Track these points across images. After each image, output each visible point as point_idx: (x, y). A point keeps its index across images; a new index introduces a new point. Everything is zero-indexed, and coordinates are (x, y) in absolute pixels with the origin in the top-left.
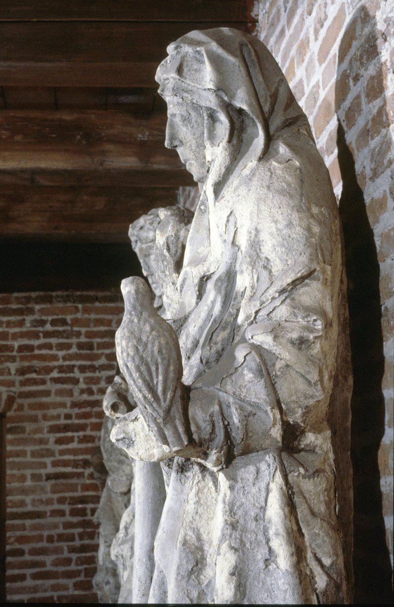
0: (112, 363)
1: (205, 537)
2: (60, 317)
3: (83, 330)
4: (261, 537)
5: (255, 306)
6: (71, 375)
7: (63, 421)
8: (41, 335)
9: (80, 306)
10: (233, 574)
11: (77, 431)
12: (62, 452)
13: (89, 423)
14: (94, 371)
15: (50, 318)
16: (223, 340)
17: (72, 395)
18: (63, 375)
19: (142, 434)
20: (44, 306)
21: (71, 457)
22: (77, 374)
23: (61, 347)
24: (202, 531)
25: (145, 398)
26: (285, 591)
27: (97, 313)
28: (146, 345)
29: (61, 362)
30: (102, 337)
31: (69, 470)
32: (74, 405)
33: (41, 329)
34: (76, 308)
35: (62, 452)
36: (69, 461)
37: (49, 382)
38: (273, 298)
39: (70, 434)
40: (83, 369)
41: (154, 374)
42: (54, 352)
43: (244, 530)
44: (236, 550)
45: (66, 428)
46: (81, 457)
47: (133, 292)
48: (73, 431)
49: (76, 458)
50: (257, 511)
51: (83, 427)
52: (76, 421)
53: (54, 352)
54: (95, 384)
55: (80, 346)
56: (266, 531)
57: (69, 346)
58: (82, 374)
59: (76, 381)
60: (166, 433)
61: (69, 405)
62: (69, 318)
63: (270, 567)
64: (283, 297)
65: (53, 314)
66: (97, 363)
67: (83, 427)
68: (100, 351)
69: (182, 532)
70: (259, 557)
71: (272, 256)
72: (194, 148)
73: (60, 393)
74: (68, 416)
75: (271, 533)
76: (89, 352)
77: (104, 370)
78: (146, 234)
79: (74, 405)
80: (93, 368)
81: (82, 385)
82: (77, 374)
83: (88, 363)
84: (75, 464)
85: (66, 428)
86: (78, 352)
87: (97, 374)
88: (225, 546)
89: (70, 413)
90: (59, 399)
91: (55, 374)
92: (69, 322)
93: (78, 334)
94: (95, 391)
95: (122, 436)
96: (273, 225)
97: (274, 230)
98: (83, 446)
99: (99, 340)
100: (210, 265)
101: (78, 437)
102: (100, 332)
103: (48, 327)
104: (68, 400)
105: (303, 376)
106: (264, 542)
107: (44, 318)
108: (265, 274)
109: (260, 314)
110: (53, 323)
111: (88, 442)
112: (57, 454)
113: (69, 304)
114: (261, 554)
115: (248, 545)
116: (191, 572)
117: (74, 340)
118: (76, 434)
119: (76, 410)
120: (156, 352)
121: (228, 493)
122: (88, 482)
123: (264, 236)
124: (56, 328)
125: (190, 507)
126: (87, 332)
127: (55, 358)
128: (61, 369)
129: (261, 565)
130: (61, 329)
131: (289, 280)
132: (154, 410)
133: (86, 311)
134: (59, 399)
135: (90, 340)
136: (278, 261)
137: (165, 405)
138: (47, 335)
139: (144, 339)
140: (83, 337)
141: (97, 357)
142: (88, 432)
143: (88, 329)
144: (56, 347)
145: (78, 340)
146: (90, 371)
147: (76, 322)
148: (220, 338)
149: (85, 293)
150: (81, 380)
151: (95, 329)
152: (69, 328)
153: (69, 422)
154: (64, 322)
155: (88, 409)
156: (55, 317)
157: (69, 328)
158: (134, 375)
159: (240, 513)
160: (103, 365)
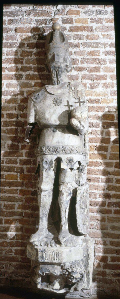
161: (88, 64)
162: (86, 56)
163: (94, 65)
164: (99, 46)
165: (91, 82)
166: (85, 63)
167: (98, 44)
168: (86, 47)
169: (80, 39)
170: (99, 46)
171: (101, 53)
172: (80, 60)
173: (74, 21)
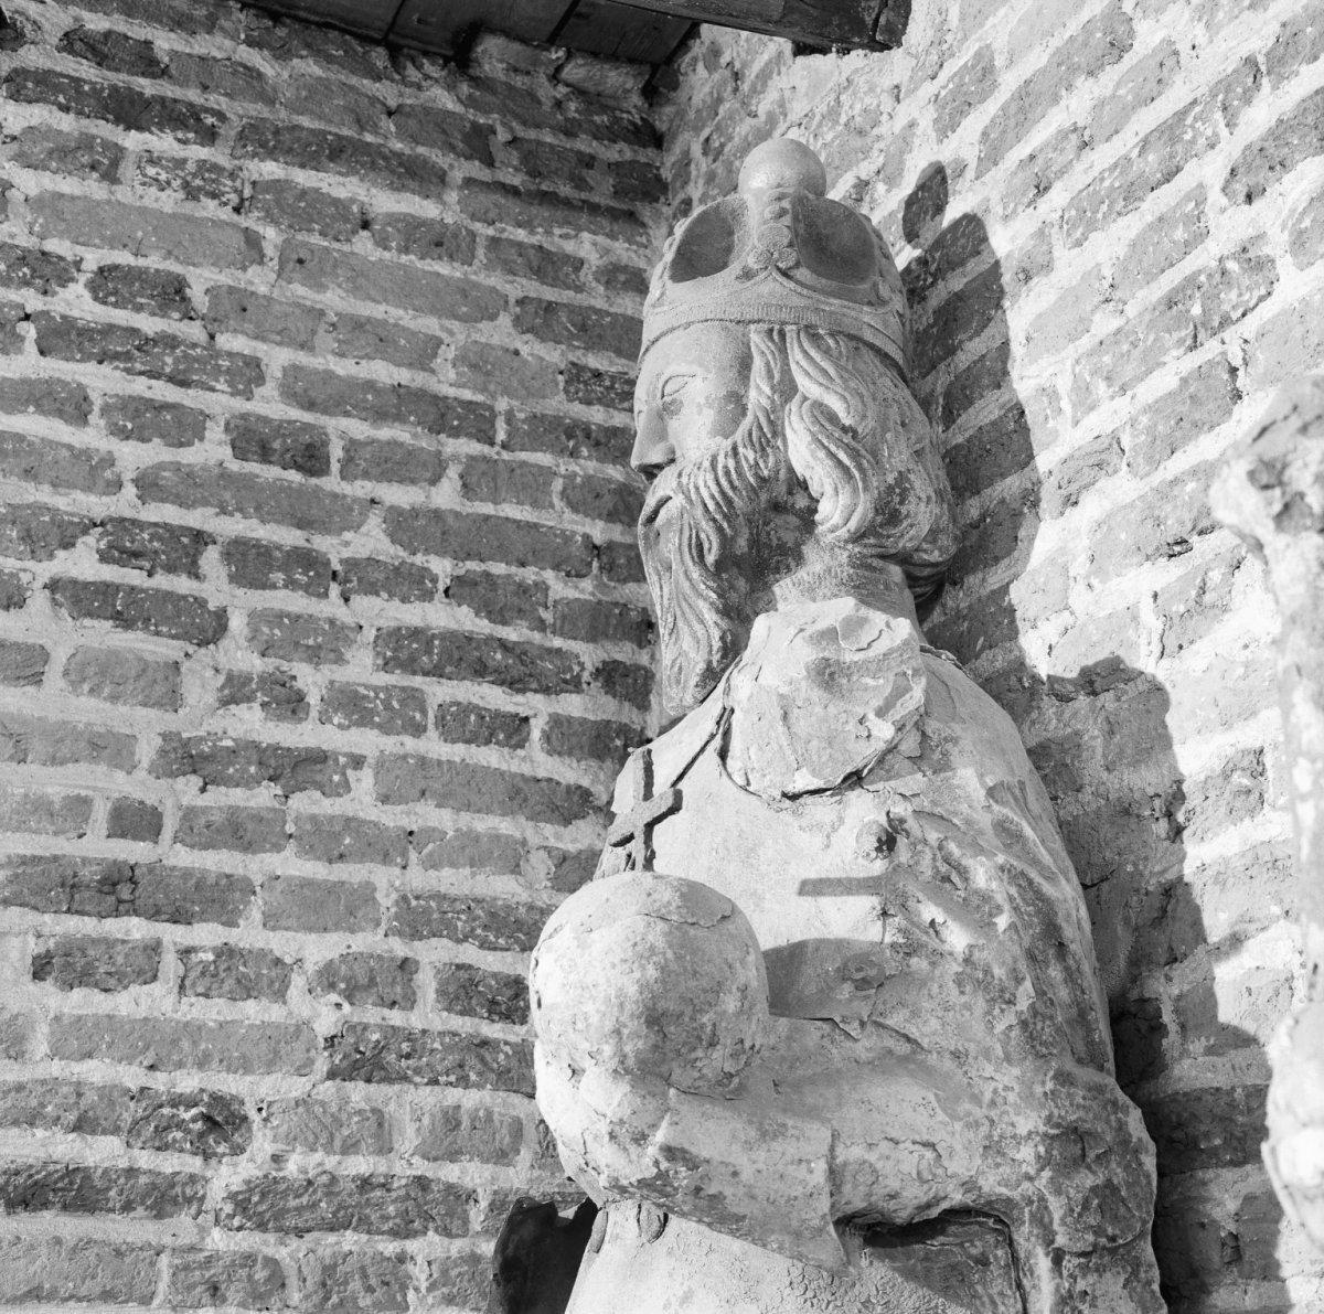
0: (419, 559)
2: (154, 262)
3: (277, 358)
6: (182, 584)
7: (98, 847)
8: (29, 331)
9: (271, 235)
11: (179, 917)
12: (77, 1039)
13: (257, 880)
14: (317, 590)
15: (93, 259)
17: (173, 700)
18: (133, 577)
20: (68, 185)
21: (132, 1076)
22: (214, 584)
23: (137, 419)
27: (356, 290)
29: (125, 503)
30: (380, 415)
31: (102, 1152)
32: (186, 758)
33: (32, 301)
34: (253, 241)
35: (77, 1039)
36: (111, 1094)
37: (39, 601)
39: (136, 928)
40: (251, 564)
42: (93, 437)
45: (117, 889)
46: (188, 1082)
48: (155, 914)
49: (160, 1082)
51: (220, 898)
52: (184, 858)
53: (93, 437)
54: (314, 656)
55: (251, 440)
57: (187, 427)
58: (240, 592)
59: (209, 628)
61: (146, 751)
62: (201, 282)
65: (113, 243)
66: (333, 548)
67: (220, 898)
68: (361, 489)
73: (94, 673)
74: (135, 821)
76: (294, 476)
77: (372, 589)
79: (186, 758)
80: (311, 570)
81: (238, 654)
82: (214, 584)
83: (289, 537)
84: (155, 1121)
85: (117, 889)
86: (235, 466)
87: (331, 607)
89: (151, 800)
90: (89, 710)
91: (83, 563)
92: (197, 294)
93: (248, 374)
94: (313, 699)
98: (211, 1011)
99: (359, 429)
101: (186, 952)
102: (370, 385)
103: (76, 302)
104: (147, 727)
107: (54, 245)
110: (107, 283)
111: (246, 989)
112: (39, 1045)
113: (209, 208)
117: (219, 402)
118: (173, 935)
119: (187, 789)
122: (218, 1240)
124: (122, 317)
126: (292, 372)
127: (95, 472)
128: (123, 543)
130: (149, 324)
133: (296, 263)
134: (89, 710)
135: (308, 417)
138: (60, 337)
140: (269, 389)
141: (343, 516)
142: (249, 934)
143: (303, 358)
144: (105, 410)
145: (240, 405)
146: (291, 584)
147: (237, 307)
149: (304, 178)
150: (237, 622)
151: (344, 368)
152: (194, 331)
153: (135, 851)
154: (172, 294)
155: (264, 796)
156: (124, 258)
157: (194, 331)
160: (371, 561)
161: (1123, 390)
162: (1105, 324)
163: (1175, 368)
164: (1187, 137)
165: (1166, 574)
166: (1101, 388)
167: (1170, 130)
168: (1092, 226)
169: (1042, 189)
170: (1187, 137)
171: (1215, 197)
172: (1064, 385)
173: (999, 62)
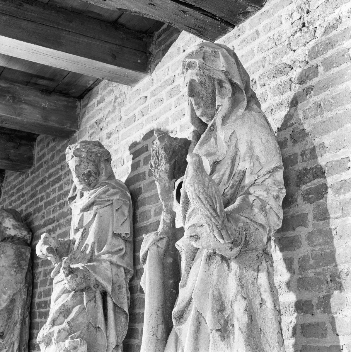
1: (222, 293)
4: (256, 292)
5: (254, 177)
10: (246, 310)
16: (231, 194)
19: (205, 234)
24: (221, 290)
25: (211, 214)
26: (272, 319)
28: (208, 188)
38: (264, 175)
41: (215, 204)
43: (247, 289)
44: (245, 299)
47: (198, 160)
50: (253, 280)
56: (258, 290)
60: (222, 233)
63: (263, 307)
64: (269, 175)
69: (211, 290)
70: (257, 302)
71: (260, 155)
72: (204, 98)
75: (262, 290)
78: (80, 153)
88: (239, 297)
95: (194, 234)
96: (260, 140)
97: (261, 143)
100: (219, 156)
105: (276, 214)
106: (258, 295)
108: (257, 163)
109: (257, 181)
114: (257, 301)
115: (250, 296)
116: (219, 311)
120: (214, 192)
121: (238, 270)
123: (255, 145)
125: (215, 278)
129: (258, 306)
131: (272, 167)
132: (216, 220)
136: (263, 158)
137: (222, 219)
139: (207, 185)
148: (229, 193)
158: (204, 202)
159: (244, 280)
